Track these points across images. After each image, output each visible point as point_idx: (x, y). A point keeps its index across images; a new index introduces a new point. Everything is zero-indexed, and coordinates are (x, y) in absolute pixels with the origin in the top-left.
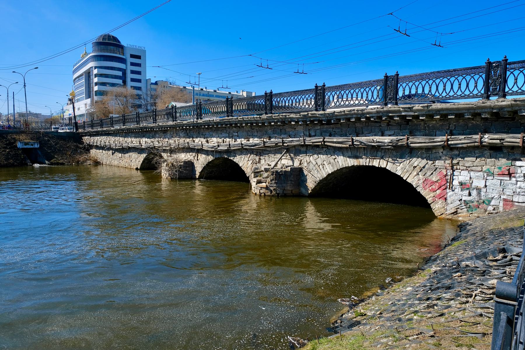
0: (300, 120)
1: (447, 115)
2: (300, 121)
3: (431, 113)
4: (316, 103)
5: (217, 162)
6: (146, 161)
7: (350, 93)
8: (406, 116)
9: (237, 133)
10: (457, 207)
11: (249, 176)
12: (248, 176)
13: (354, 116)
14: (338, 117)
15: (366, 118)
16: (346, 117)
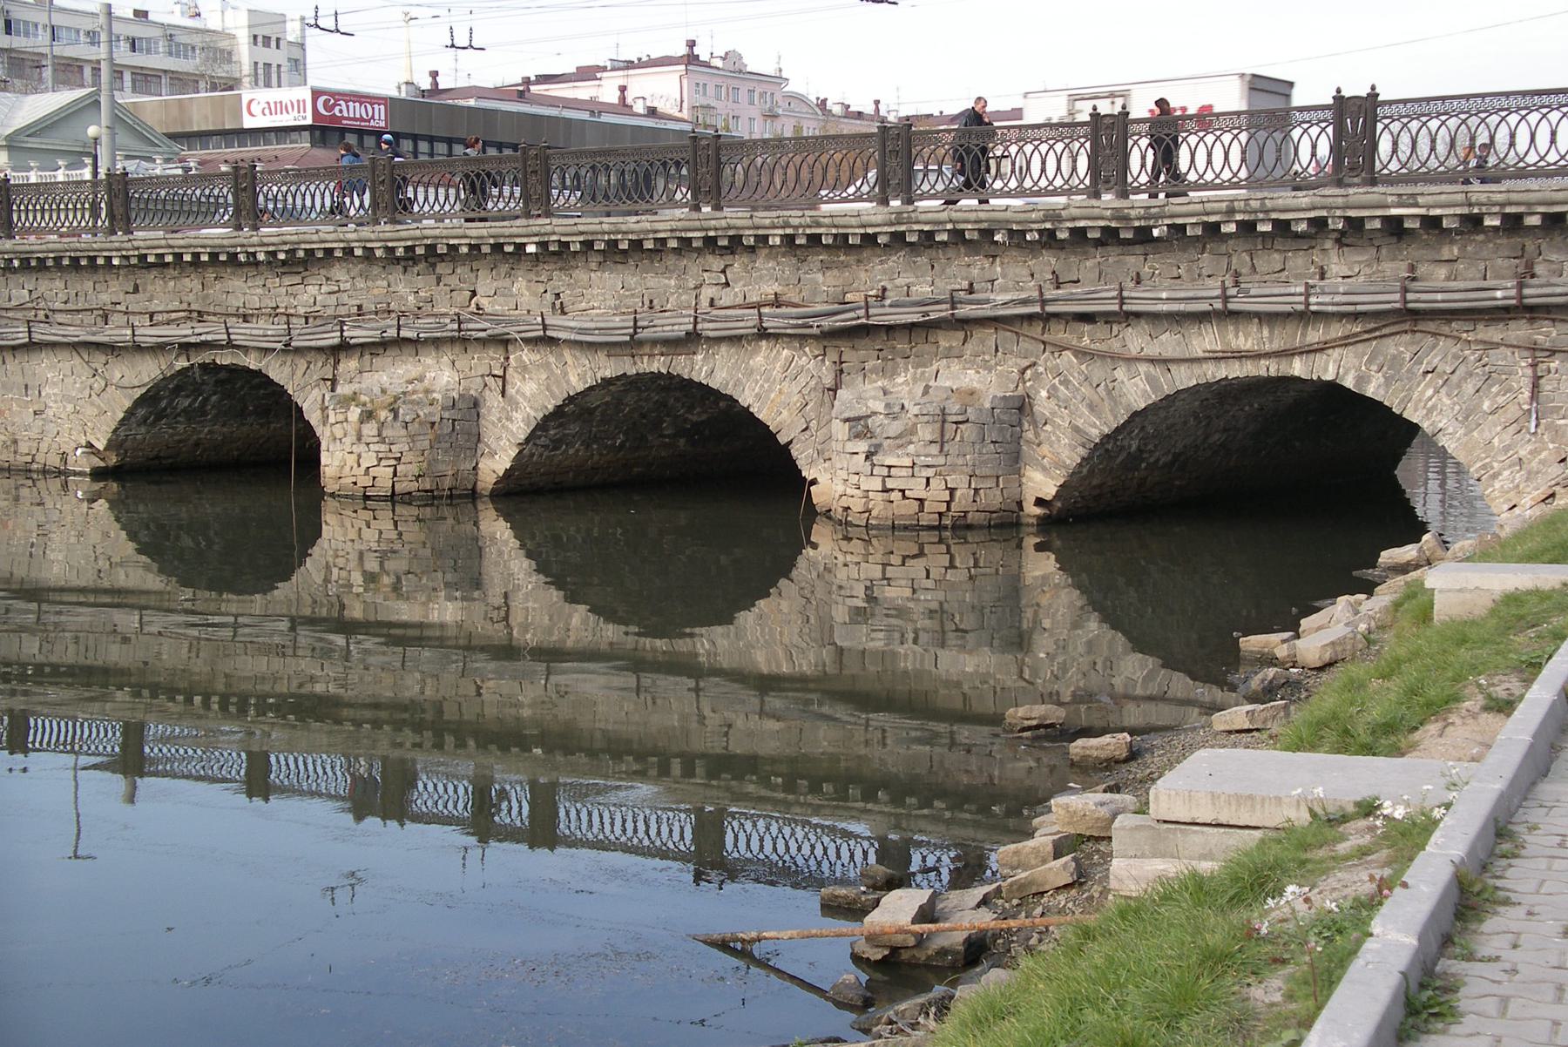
0: (1035, 226)
1: (1519, 217)
2: (1031, 230)
3: (1476, 211)
4: (1093, 168)
5: (594, 401)
6: (141, 412)
7: (1218, 142)
8: (1399, 219)
9: (723, 272)
10: (1553, 482)
11: (791, 442)
12: (782, 439)
13: (1239, 217)
14: (1180, 221)
15: (1276, 222)
16: (1205, 219)
